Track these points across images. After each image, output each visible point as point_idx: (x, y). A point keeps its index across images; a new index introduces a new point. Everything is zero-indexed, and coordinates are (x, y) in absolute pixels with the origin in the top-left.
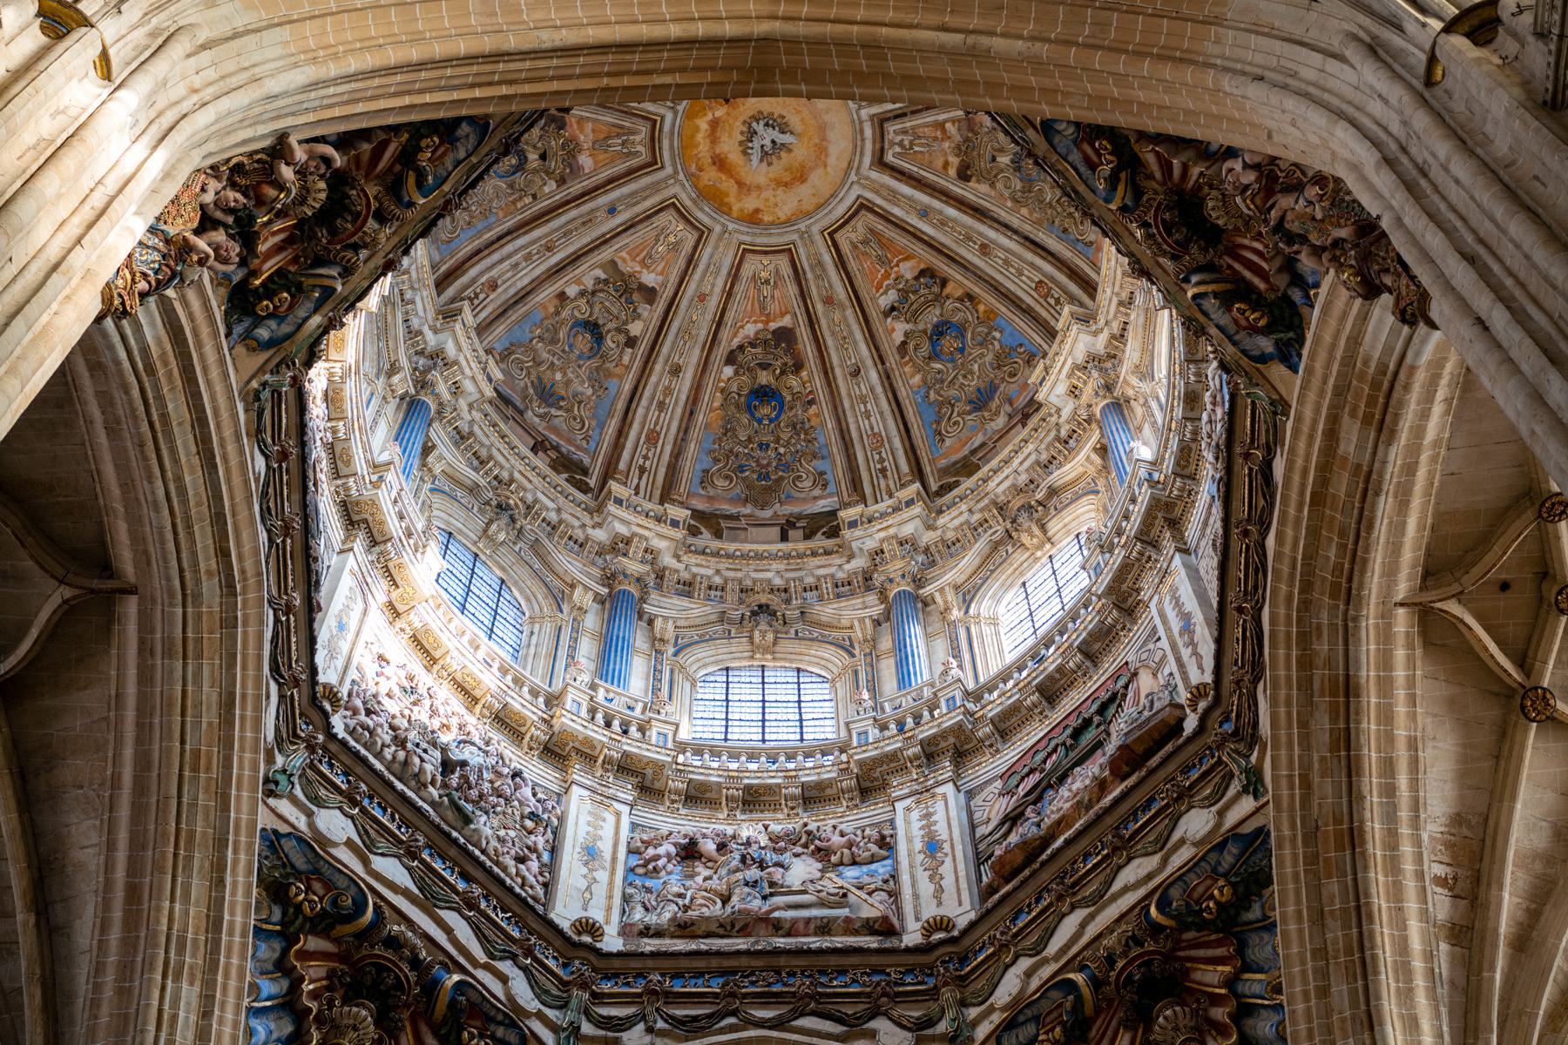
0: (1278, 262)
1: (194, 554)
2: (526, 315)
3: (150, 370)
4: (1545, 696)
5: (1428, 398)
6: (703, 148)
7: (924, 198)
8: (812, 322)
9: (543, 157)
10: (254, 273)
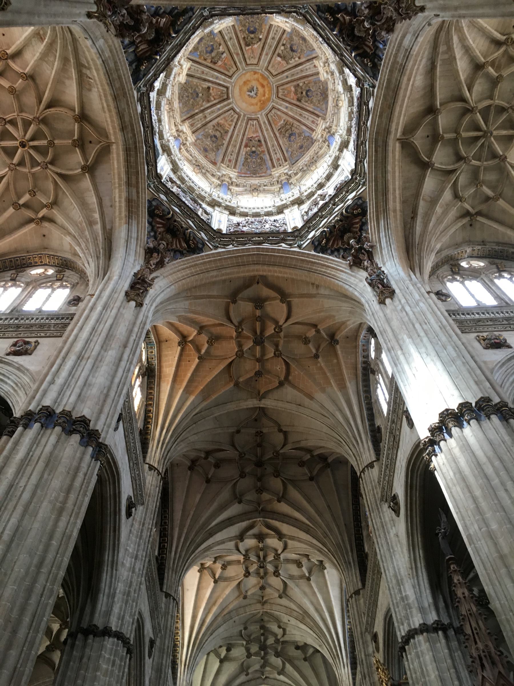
0: (155, 228)
1: (382, 154)
2: (308, 56)
3: (384, 210)
4: (76, 121)
5: (120, 207)
6: (267, 90)
7: (218, 81)
8: (241, 49)
9: (302, 93)
10: (361, 220)
